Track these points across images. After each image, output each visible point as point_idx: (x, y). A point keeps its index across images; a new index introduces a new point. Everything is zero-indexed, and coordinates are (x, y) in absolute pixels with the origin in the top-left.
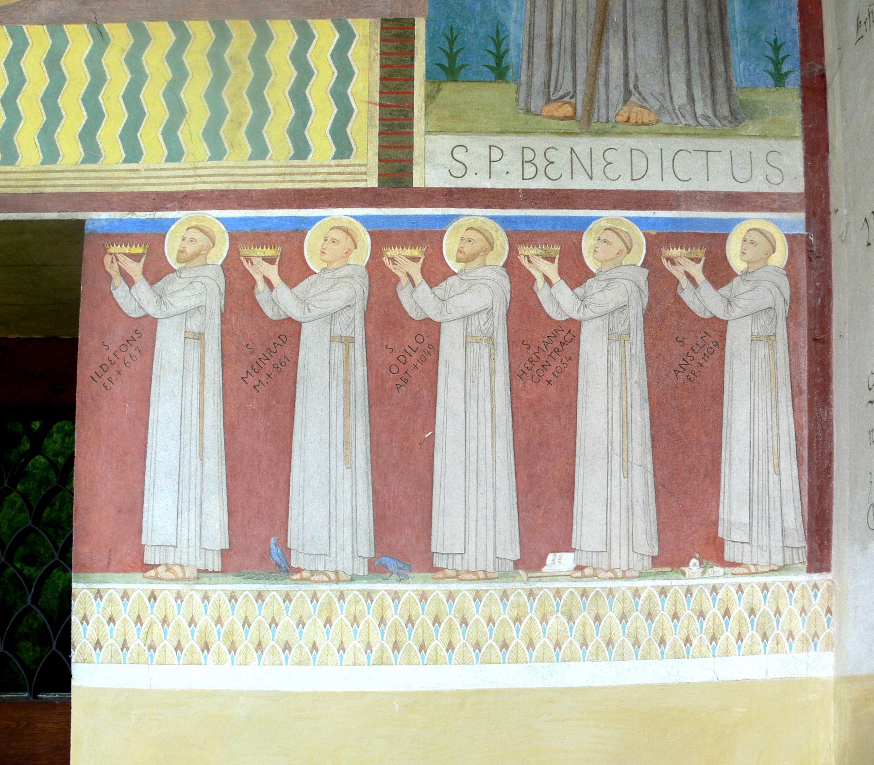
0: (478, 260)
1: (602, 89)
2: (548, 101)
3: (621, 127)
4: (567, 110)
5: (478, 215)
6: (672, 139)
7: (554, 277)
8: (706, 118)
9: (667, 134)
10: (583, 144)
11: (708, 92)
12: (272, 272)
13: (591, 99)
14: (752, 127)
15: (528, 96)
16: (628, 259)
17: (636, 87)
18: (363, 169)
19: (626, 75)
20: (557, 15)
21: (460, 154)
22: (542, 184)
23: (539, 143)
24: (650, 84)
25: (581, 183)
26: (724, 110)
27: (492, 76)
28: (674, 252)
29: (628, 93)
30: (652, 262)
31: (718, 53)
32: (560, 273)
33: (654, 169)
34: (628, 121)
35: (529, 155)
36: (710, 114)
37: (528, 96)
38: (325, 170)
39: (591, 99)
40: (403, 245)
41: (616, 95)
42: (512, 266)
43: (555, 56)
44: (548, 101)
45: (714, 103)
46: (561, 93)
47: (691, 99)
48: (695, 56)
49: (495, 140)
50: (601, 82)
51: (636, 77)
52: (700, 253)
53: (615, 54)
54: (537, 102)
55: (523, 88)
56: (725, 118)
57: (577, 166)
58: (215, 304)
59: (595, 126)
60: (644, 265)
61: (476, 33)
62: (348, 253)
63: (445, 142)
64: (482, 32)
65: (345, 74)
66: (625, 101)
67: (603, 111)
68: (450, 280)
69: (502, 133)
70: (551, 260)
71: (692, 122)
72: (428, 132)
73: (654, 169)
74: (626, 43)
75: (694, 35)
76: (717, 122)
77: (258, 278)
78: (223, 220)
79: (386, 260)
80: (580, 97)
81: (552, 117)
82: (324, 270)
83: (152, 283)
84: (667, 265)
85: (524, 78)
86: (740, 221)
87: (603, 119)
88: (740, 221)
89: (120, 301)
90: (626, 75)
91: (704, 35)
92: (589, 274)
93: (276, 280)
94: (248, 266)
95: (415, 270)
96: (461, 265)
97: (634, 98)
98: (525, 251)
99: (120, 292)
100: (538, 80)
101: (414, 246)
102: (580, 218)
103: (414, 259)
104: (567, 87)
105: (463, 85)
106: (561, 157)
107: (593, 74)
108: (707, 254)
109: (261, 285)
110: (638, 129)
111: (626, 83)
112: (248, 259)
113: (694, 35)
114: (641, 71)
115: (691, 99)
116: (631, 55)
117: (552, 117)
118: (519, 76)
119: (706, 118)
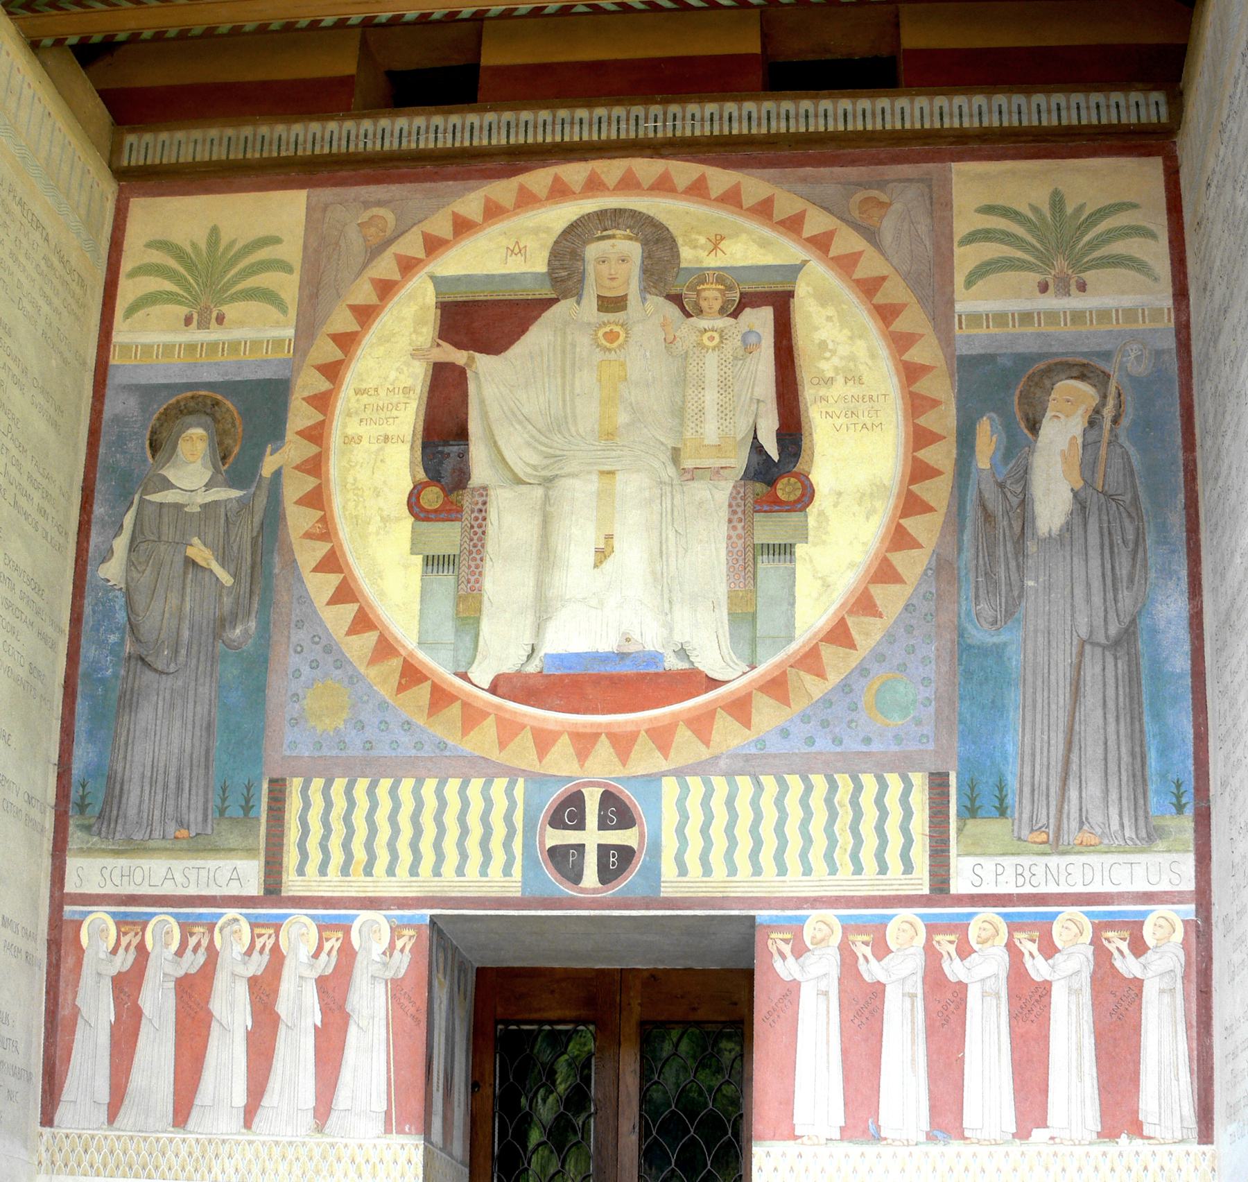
0: (990, 943)
1: (1065, 821)
2: (1032, 831)
3: (1077, 848)
4: (1043, 837)
5: (989, 913)
6: (1109, 856)
7: (1036, 953)
8: (1131, 839)
9: (1106, 852)
10: (1053, 861)
11: (1133, 821)
12: (868, 951)
13: (1059, 829)
14: (1161, 845)
15: (1020, 828)
16: (1081, 940)
17: (1087, 819)
18: (920, 882)
19: (1081, 810)
20: (1038, 767)
21: (978, 870)
22: (1027, 889)
23: (1025, 861)
24: (1096, 817)
25: (1052, 888)
26: (1143, 834)
27: (997, 814)
28: (1110, 934)
29: (1081, 823)
30: (1096, 942)
31: (1140, 790)
32: (1040, 950)
33: (1098, 878)
34: (1081, 843)
35: (1020, 870)
36: (1134, 837)
37: (1020, 828)
38: (899, 882)
39: (1059, 829)
40: (945, 933)
41: (1074, 824)
42: (1011, 946)
43: (1036, 799)
44: (1032, 831)
45: (1137, 830)
46: (1040, 825)
47: (1122, 826)
48: (1124, 794)
49: (999, 859)
50: (1065, 816)
51: (1087, 811)
52: (1126, 934)
53: (1073, 794)
54: (1025, 833)
55: (1016, 822)
56: (1143, 839)
57: (1049, 877)
58: (835, 972)
59: (1061, 848)
60: (1090, 944)
61: (987, 782)
62: (912, 938)
63: (969, 861)
64: (991, 783)
65: (908, 814)
66: (1080, 828)
67: (1066, 837)
68: (974, 955)
69: (1003, 854)
70: (1034, 941)
71: (1122, 843)
72: (959, 855)
73: (1098, 878)
74: (1080, 787)
75: (1124, 778)
76: (1138, 842)
77: (860, 955)
78: (838, 917)
79: (934, 943)
80: (1052, 827)
81: (1035, 843)
82: (898, 949)
83: (797, 959)
84: (1106, 943)
85: (1017, 815)
86: (1152, 911)
87: (1066, 843)
88: (1152, 911)
89: (778, 970)
90: (1081, 810)
91: (1131, 779)
92: (1057, 950)
93: (870, 957)
94: (853, 947)
95: (952, 949)
96: (980, 946)
97: (1086, 827)
98: (1017, 935)
99: (778, 964)
100: (1026, 816)
101: (951, 934)
102: (1051, 913)
103: (951, 942)
104: (1043, 821)
105: (979, 821)
106: (1039, 871)
107: (1060, 811)
108: (1131, 934)
109: (861, 960)
110: (1086, 849)
111: (1081, 816)
112: (853, 943)
113: (1124, 778)
114: (1090, 806)
115: (1122, 826)
116: (1084, 795)
117: (1035, 843)
118: (1013, 812)
119: (1131, 839)
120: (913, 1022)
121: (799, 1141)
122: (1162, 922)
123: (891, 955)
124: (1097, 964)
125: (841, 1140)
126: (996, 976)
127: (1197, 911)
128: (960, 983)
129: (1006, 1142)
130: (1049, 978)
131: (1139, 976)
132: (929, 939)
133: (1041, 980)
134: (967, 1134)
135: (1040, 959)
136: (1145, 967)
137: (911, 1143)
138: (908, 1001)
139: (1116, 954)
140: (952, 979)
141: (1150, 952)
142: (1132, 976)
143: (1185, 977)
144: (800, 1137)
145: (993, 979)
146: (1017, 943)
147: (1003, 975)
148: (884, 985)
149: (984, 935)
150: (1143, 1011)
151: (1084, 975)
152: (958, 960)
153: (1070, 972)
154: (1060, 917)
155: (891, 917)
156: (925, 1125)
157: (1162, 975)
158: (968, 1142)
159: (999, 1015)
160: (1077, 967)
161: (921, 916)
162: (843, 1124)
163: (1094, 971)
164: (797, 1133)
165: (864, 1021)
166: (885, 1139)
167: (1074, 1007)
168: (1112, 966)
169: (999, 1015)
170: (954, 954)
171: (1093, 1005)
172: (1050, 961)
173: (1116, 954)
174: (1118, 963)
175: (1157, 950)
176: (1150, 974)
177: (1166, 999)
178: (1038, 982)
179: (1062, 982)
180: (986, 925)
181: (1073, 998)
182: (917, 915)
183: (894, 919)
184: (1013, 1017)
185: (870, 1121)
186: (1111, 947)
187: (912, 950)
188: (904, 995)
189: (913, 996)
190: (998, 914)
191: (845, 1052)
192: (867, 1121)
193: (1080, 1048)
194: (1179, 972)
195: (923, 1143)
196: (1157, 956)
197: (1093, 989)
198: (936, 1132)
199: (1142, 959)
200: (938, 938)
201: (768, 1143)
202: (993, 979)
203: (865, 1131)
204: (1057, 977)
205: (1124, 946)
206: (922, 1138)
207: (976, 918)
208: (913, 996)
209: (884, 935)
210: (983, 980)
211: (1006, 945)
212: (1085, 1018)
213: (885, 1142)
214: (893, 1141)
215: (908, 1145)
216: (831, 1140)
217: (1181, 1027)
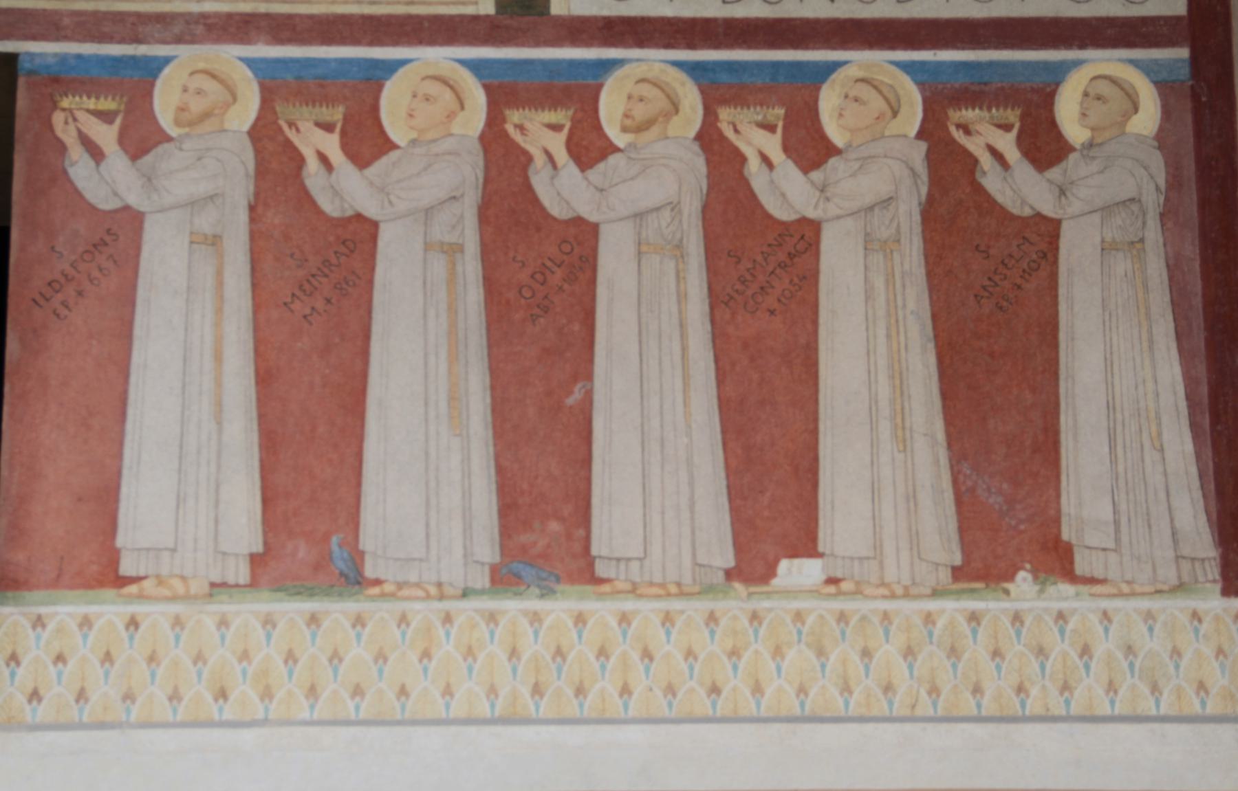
62: (451, 116)
79: (510, 128)
82: (413, 142)
95: (557, 144)
103: (556, 128)
120: (452, 310)
121: (133, 589)
122: (1104, 88)
123: (394, 155)
124: (936, 180)
125: (254, 584)
126: (675, 207)
127: (1194, 60)
128: (578, 221)
129: (708, 590)
130: (811, 214)
131: (1048, 210)
132: (495, 120)
133: (793, 217)
134: (601, 570)
135: (788, 171)
136: (1062, 192)
137: (448, 590)
138: (439, 266)
139: (986, 160)
140: (556, 210)
141: (1073, 157)
142: (1027, 212)
143: (1167, 215)
144: (137, 579)
145: (666, 214)
146: (729, 133)
147: (692, 207)
148: (375, 225)
149: (640, 112)
150: (1062, 291)
151: (903, 208)
152: (573, 169)
153: (868, 200)
154: (839, 75)
155: (392, 67)
156: (487, 551)
157: (1107, 210)
158: (606, 588)
159: (682, 297)
160: (885, 189)
161: (475, 67)
162: (258, 547)
163: (931, 199)
164: (127, 567)
165: (320, 305)
166: (377, 582)
167: (879, 283)
168: (979, 190)
169: (682, 297)
170: (561, 156)
171: (930, 275)
172: (816, 175)
173: (986, 160)
174: (992, 181)
175: (1094, 152)
176: (1075, 207)
177: (1122, 264)
178: (783, 223)
179: (849, 223)
180: (646, 90)
181: (877, 259)
182: (463, 62)
183: (401, 72)
184: (717, 300)
185: (335, 540)
186: (974, 145)
187: (447, 145)
188: (427, 247)
189: (453, 251)
190: (677, 64)
191: (265, 378)
192: (326, 538)
193: (898, 378)
194: (1153, 201)
195: (481, 592)
196: (1095, 167)
197: (927, 240)
198: (516, 566)
199: (1054, 173)
200: (514, 116)
201: (38, 595)
202: (666, 214)
203: (321, 564)
204: (833, 210)
205: (1007, 143)
206: (482, 580)
207: (619, 73)
208: (453, 251)
209: (375, 109)
210: (639, 216)
211: (699, 137)
212: (911, 305)
213: (375, 590)
214: (400, 585)
215: (441, 597)
216: (224, 585)
217: (1164, 328)
